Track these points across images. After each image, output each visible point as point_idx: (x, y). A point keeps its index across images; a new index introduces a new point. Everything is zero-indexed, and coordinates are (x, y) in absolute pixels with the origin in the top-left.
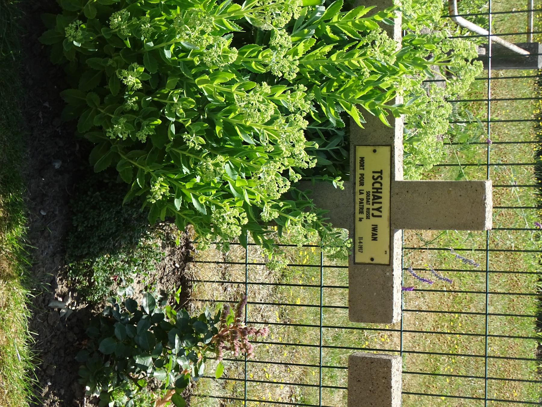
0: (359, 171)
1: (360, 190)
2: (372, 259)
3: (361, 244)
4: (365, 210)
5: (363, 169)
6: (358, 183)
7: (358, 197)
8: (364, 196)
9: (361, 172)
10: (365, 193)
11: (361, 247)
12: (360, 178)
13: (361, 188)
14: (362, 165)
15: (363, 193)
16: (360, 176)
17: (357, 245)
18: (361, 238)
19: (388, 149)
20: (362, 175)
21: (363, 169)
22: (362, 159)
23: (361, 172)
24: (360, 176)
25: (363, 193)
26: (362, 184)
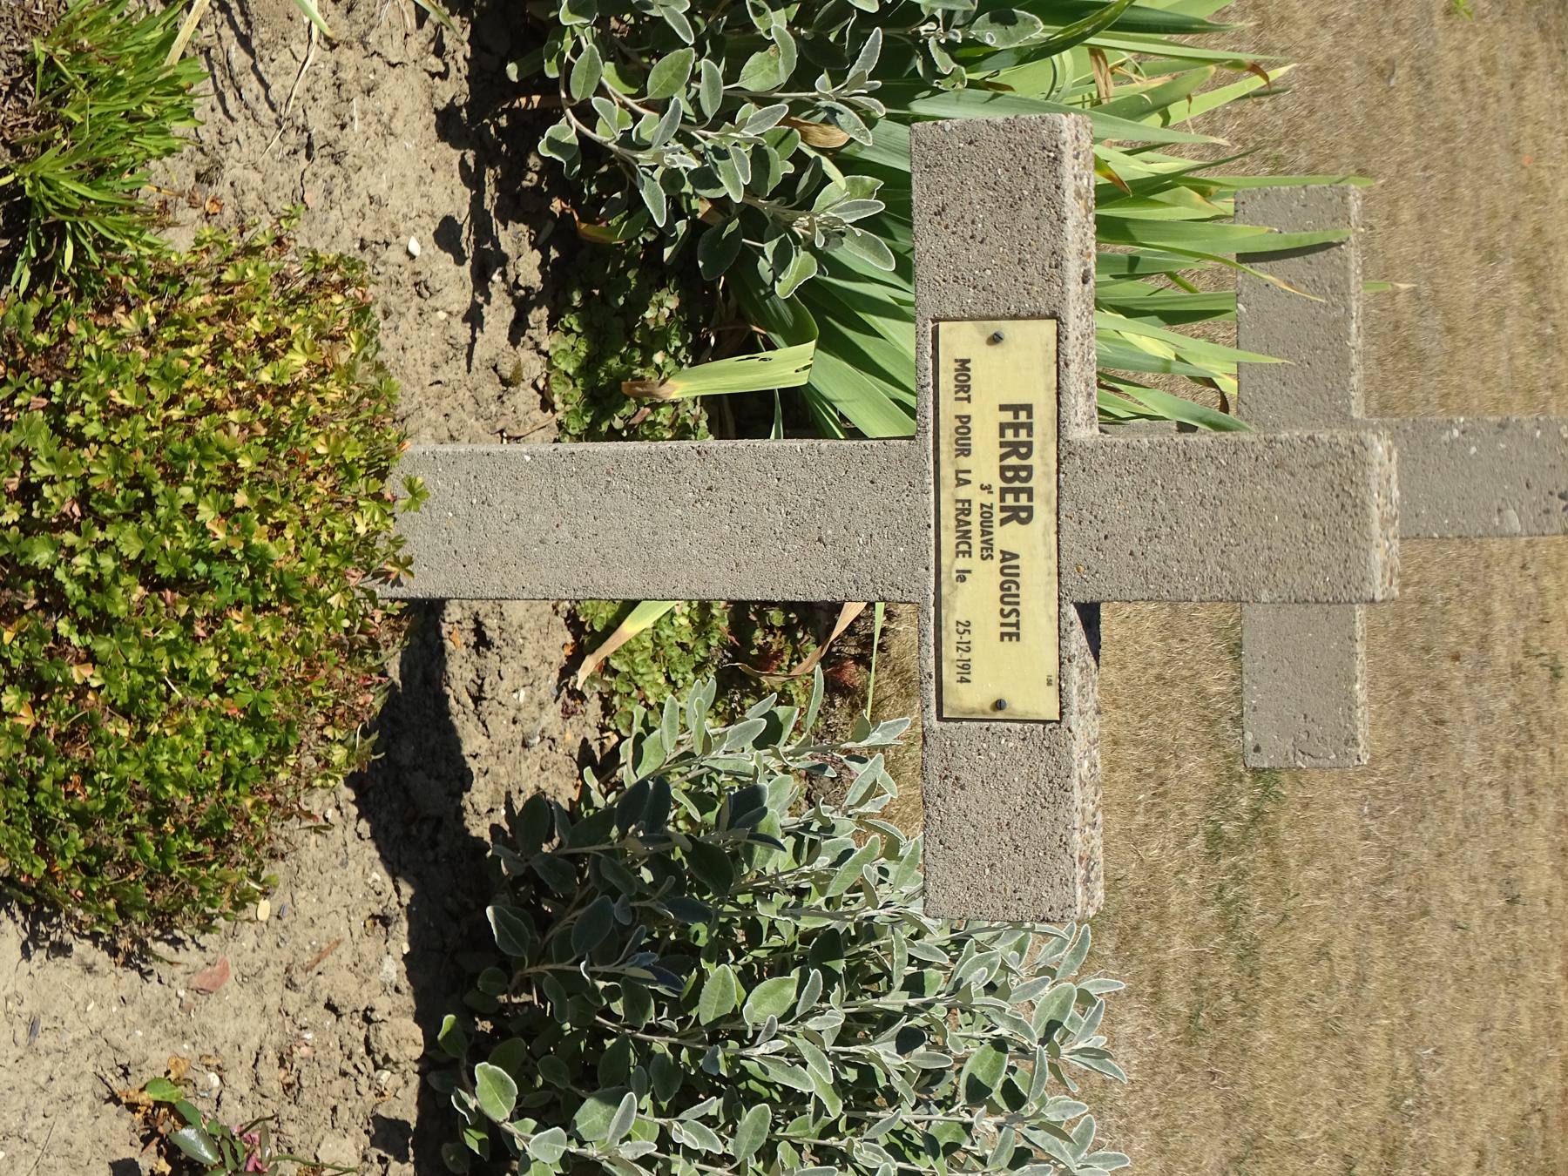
2: (999, 705)
5: (968, 399)
9: (965, 408)
11: (965, 666)
12: (957, 429)
13: (964, 463)
14: (963, 387)
15: (968, 482)
19: (1051, 325)
20: (965, 420)
21: (968, 399)
22: (964, 365)
23: (965, 408)
25: (968, 482)
26: (964, 450)
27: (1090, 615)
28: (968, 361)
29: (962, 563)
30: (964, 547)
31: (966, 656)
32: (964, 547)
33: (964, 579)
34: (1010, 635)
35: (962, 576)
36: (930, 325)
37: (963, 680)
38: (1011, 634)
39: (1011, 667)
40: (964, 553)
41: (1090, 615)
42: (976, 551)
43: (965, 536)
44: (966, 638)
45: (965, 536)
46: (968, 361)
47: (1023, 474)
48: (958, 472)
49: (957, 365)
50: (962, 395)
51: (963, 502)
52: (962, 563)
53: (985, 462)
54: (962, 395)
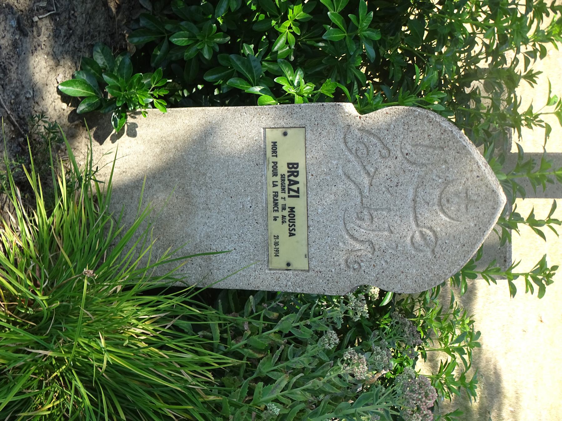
1: (273, 182)
3: (277, 247)
4: (280, 207)
5: (276, 156)
8: (278, 189)
9: (275, 159)
10: (279, 184)
11: (277, 251)
13: (275, 179)
15: (277, 185)
16: (273, 164)
20: (275, 163)
21: (276, 156)
22: (274, 144)
23: (275, 159)
24: (273, 164)
25: (277, 185)
26: (275, 174)
28: (276, 142)
29: (276, 214)
30: (276, 208)
32: (276, 208)
35: (275, 219)
40: (276, 210)
42: (280, 209)
43: (276, 205)
44: (277, 240)
45: (276, 205)
46: (276, 142)
48: (273, 182)
49: (272, 144)
50: (274, 154)
51: (275, 192)
52: (276, 214)
54: (274, 154)
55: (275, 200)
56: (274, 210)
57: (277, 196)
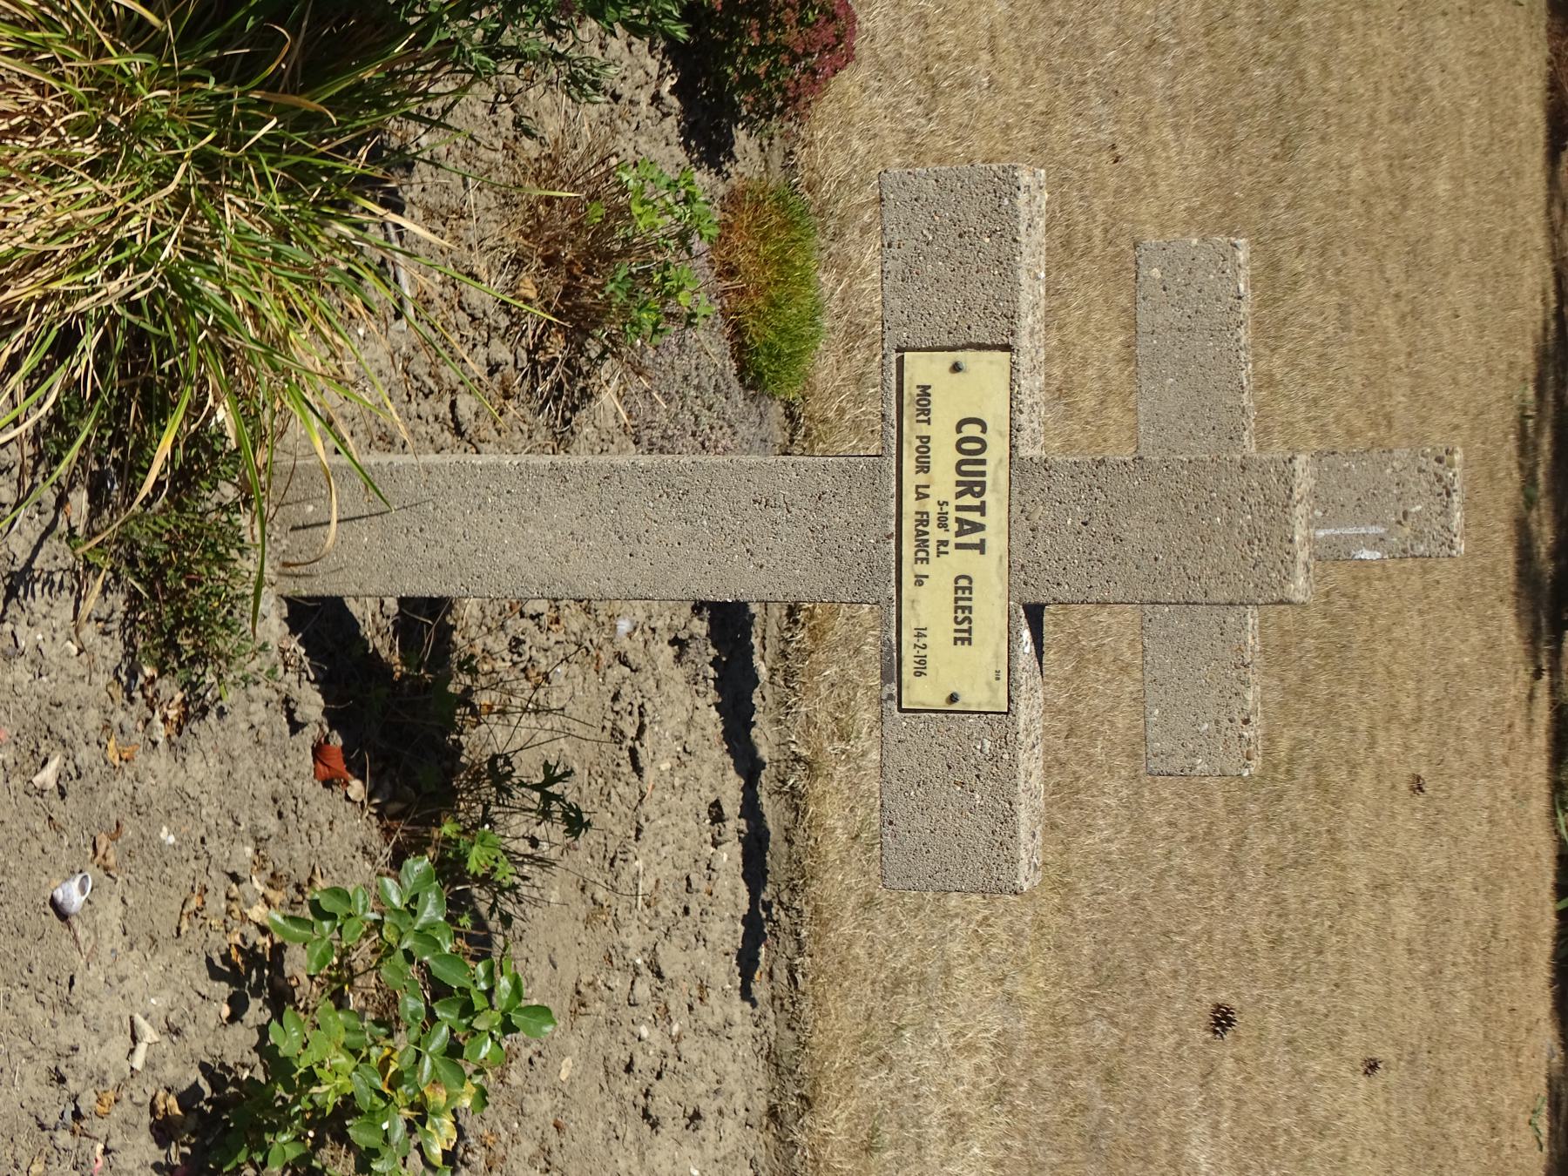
0: (911, 430)
2: (953, 698)
3: (922, 652)
4: (932, 550)
5: (928, 422)
6: (909, 464)
7: (910, 504)
9: (924, 430)
13: (922, 479)
14: (924, 411)
15: (927, 496)
16: (918, 443)
17: (909, 654)
18: (920, 634)
20: (925, 440)
21: (928, 422)
22: (925, 390)
23: (924, 430)
24: (918, 443)
25: (927, 496)
26: (923, 467)
27: (1035, 614)
30: (922, 555)
31: (922, 652)
32: (922, 555)
33: (921, 584)
34: (963, 640)
35: (919, 580)
36: (894, 357)
37: (918, 674)
38: (964, 638)
39: (962, 666)
40: (922, 560)
41: (1035, 614)
43: (922, 544)
45: (922, 544)
47: (977, 489)
49: (918, 391)
50: (922, 417)
51: (922, 513)
52: (922, 569)
53: (943, 480)
54: (922, 417)
55: (920, 533)
56: (917, 560)
57: (926, 523)
